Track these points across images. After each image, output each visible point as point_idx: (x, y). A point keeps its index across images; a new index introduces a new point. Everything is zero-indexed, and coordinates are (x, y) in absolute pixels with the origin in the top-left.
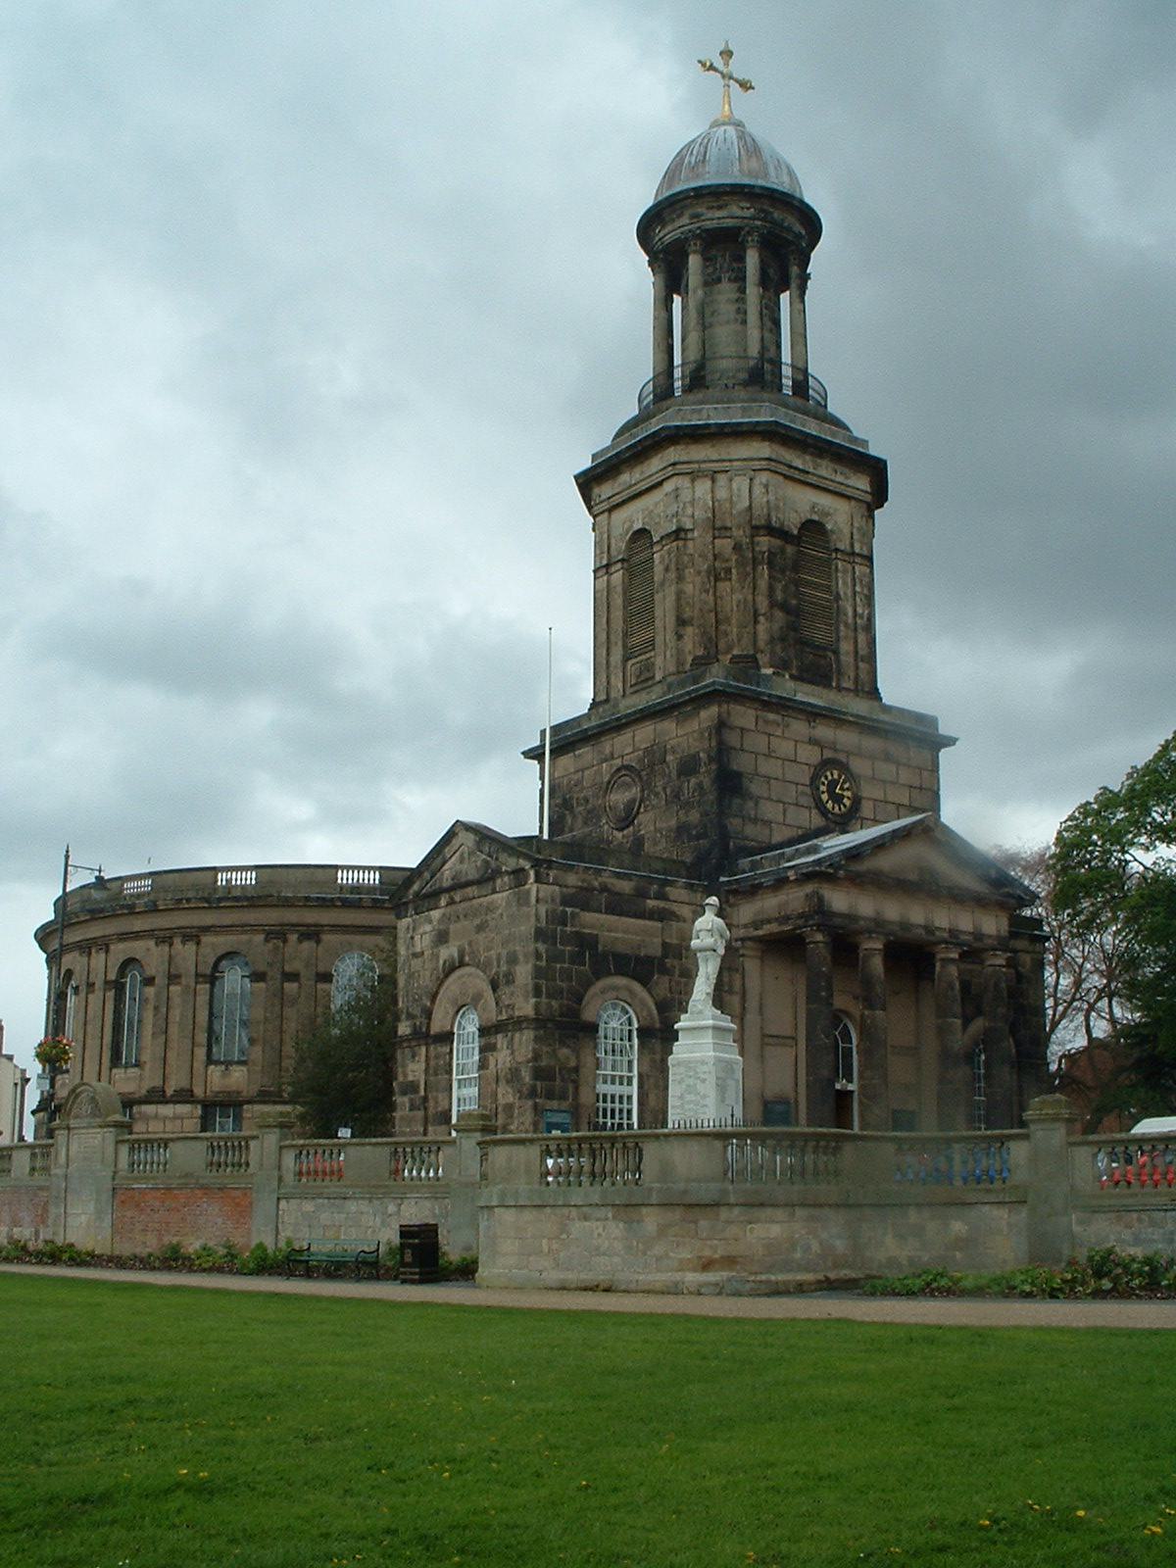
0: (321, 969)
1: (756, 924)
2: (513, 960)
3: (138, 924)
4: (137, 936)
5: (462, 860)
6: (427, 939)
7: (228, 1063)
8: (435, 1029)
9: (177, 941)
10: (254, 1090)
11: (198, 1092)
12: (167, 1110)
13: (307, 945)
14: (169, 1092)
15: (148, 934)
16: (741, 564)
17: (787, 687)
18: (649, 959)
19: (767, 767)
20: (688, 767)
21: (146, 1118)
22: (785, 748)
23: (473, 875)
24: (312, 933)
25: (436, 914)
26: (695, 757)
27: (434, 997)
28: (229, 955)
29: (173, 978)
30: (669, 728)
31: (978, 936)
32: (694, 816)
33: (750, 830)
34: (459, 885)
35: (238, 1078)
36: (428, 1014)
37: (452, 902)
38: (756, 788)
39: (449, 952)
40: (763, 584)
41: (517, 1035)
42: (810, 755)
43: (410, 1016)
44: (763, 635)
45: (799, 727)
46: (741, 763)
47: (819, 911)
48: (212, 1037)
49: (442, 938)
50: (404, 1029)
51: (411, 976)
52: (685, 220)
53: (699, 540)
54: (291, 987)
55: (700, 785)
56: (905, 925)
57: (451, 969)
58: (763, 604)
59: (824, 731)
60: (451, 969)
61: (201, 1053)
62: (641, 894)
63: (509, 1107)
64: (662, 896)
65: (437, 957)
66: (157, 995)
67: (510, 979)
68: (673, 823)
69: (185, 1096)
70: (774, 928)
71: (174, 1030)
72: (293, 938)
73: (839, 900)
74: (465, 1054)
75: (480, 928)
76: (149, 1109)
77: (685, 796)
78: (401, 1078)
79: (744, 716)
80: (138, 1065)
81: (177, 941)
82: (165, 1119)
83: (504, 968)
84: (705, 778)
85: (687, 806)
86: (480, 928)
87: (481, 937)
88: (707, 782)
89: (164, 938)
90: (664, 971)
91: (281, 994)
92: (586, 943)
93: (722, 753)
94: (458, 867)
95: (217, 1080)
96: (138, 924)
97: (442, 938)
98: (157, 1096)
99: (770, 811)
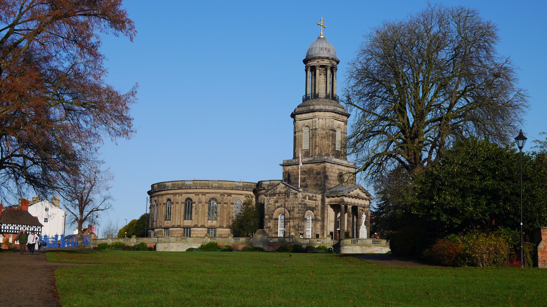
0: (231, 202)
1: (330, 202)
2: (294, 207)
3: (190, 191)
4: (190, 193)
6: (273, 202)
7: (212, 220)
9: (200, 195)
10: (218, 225)
11: (206, 226)
12: (200, 229)
13: (229, 197)
14: (199, 226)
15: (194, 193)
16: (327, 136)
17: (334, 160)
18: (313, 208)
19: (332, 174)
20: (318, 173)
21: (194, 231)
22: (334, 170)
24: (230, 195)
26: (320, 172)
28: (213, 199)
29: (200, 202)
30: (314, 166)
31: (365, 205)
32: (319, 183)
33: (329, 185)
34: (280, 193)
35: (215, 223)
36: (273, 215)
38: (330, 178)
40: (331, 140)
42: (338, 172)
44: (331, 150)
45: (336, 166)
46: (328, 174)
47: (343, 201)
48: (209, 214)
49: (276, 202)
50: (266, 217)
51: (268, 208)
52: (315, 62)
53: (319, 131)
54: (225, 205)
55: (321, 178)
56: (355, 203)
57: (278, 207)
58: (330, 144)
59: (340, 167)
60: (278, 207)
61: (206, 218)
62: (313, 196)
64: (316, 197)
66: (196, 206)
67: (293, 210)
68: (315, 183)
69: (203, 226)
70: (334, 203)
71: (200, 213)
72: (226, 195)
73: (346, 199)
74: (280, 223)
77: (317, 179)
79: (328, 165)
80: (191, 219)
81: (200, 195)
82: (199, 231)
84: (322, 176)
85: (318, 180)
88: (322, 177)
89: (197, 194)
90: (316, 210)
91: (223, 206)
92: (305, 205)
93: (325, 172)
95: (209, 223)
96: (190, 191)
97: (276, 202)
99: (332, 182)
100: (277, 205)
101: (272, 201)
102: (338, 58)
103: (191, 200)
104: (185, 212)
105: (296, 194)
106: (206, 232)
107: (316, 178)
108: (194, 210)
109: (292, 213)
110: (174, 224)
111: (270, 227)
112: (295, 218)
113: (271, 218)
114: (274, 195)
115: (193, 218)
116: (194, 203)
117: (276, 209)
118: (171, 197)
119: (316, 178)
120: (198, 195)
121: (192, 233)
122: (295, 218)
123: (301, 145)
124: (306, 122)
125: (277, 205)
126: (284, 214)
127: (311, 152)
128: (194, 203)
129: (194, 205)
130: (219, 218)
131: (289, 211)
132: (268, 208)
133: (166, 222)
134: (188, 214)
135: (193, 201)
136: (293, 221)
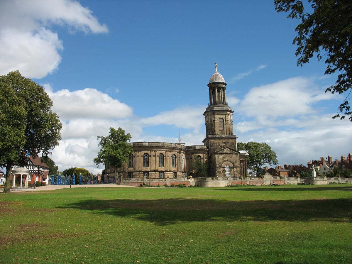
4: (163, 151)
5: (227, 151)
6: (221, 158)
8: (222, 166)
23: (229, 153)
25: (223, 155)
27: (222, 163)
29: (168, 156)
34: (226, 153)
39: (226, 159)
41: (237, 168)
49: (224, 158)
50: (217, 166)
57: (226, 161)
60: (226, 161)
63: (237, 174)
65: (223, 160)
67: (236, 163)
69: (170, 171)
75: (230, 158)
76: (166, 172)
78: (217, 171)
82: (169, 174)
86: (230, 158)
87: (231, 159)
94: (226, 151)
97: (224, 158)
98: (167, 171)
100: (224, 159)
101: (221, 157)
102: (327, 92)
103: (163, 155)
104: (159, 162)
106: (172, 174)
108: (165, 161)
109: (235, 164)
110: (152, 169)
111: (220, 172)
112: (238, 167)
113: (220, 167)
115: (165, 166)
116: (165, 156)
117: (224, 162)
118: (149, 152)
120: (167, 152)
121: (165, 174)
122: (238, 167)
124: (221, 116)
125: (224, 159)
126: (229, 165)
127: (225, 132)
128: (165, 156)
129: (165, 158)
130: (177, 166)
131: (233, 163)
132: (218, 161)
133: (144, 168)
134: (161, 163)
135: (165, 155)
136: (236, 169)
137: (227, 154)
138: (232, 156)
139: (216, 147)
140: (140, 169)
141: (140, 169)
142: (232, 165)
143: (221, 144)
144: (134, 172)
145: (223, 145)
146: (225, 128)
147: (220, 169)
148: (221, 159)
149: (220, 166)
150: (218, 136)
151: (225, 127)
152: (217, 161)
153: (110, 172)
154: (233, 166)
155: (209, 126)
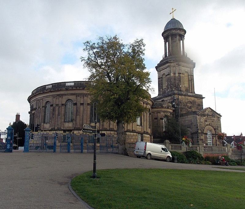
6: (203, 121)
8: (205, 132)
23: (210, 115)
30: (196, 99)
37: (208, 117)
43: (200, 130)
49: (206, 121)
51: (200, 125)
57: (207, 125)
60: (207, 125)
75: (212, 122)
76: (145, 135)
83: (216, 128)
86: (212, 122)
100: (206, 123)
101: (203, 119)
105: (219, 118)
107: (198, 108)
109: (217, 131)
110: (128, 128)
111: (202, 140)
113: (202, 133)
114: (204, 115)
115: (143, 125)
119: (198, 108)
123: (184, 84)
125: (206, 123)
127: (190, 90)
131: (215, 129)
137: (209, 116)
138: (214, 120)
139: (182, 107)
140: (111, 127)
141: (111, 127)
142: (214, 132)
143: (188, 104)
144: (102, 130)
145: (191, 105)
146: (190, 85)
147: (202, 136)
148: (203, 122)
149: (202, 132)
150: (184, 93)
151: (190, 84)
152: (199, 125)
153: (50, 129)
154: (215, 133)
155: (172, 80)
